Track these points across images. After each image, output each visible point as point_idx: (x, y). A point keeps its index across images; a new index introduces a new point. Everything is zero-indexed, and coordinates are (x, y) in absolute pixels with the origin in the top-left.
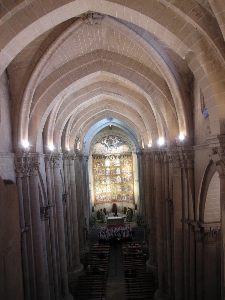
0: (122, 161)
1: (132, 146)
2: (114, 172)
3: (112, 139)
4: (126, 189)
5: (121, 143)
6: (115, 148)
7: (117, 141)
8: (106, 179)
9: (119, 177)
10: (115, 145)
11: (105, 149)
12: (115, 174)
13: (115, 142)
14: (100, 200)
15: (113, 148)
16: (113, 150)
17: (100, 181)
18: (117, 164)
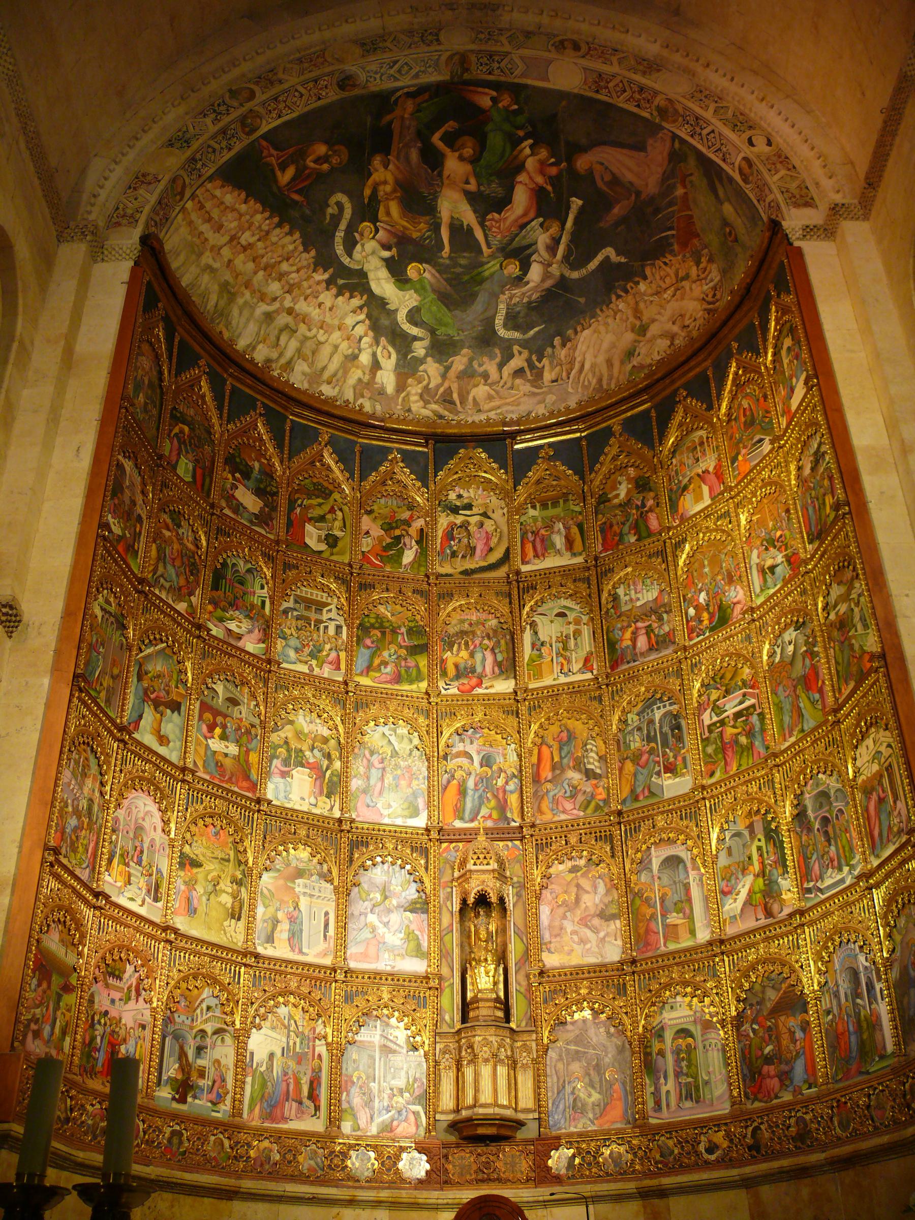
0: (623, 491)
1: (782, 159)
2: (485, 661)
3: (468, 217)
4: (725, 893)
5: (593, 265)
6: (517, 362)
7: (542, 239)
8: (346, 750)
9: (578, 726)
10: (512, 320)
11: (365, 358)
12: (505, 686)
13: (513, 268)
14: (184, 1089)
15: (491, 367)
16: (480, 391)
17: (244, 735)
18: (543, 547)
